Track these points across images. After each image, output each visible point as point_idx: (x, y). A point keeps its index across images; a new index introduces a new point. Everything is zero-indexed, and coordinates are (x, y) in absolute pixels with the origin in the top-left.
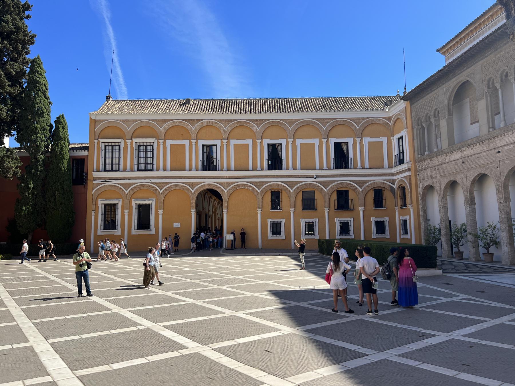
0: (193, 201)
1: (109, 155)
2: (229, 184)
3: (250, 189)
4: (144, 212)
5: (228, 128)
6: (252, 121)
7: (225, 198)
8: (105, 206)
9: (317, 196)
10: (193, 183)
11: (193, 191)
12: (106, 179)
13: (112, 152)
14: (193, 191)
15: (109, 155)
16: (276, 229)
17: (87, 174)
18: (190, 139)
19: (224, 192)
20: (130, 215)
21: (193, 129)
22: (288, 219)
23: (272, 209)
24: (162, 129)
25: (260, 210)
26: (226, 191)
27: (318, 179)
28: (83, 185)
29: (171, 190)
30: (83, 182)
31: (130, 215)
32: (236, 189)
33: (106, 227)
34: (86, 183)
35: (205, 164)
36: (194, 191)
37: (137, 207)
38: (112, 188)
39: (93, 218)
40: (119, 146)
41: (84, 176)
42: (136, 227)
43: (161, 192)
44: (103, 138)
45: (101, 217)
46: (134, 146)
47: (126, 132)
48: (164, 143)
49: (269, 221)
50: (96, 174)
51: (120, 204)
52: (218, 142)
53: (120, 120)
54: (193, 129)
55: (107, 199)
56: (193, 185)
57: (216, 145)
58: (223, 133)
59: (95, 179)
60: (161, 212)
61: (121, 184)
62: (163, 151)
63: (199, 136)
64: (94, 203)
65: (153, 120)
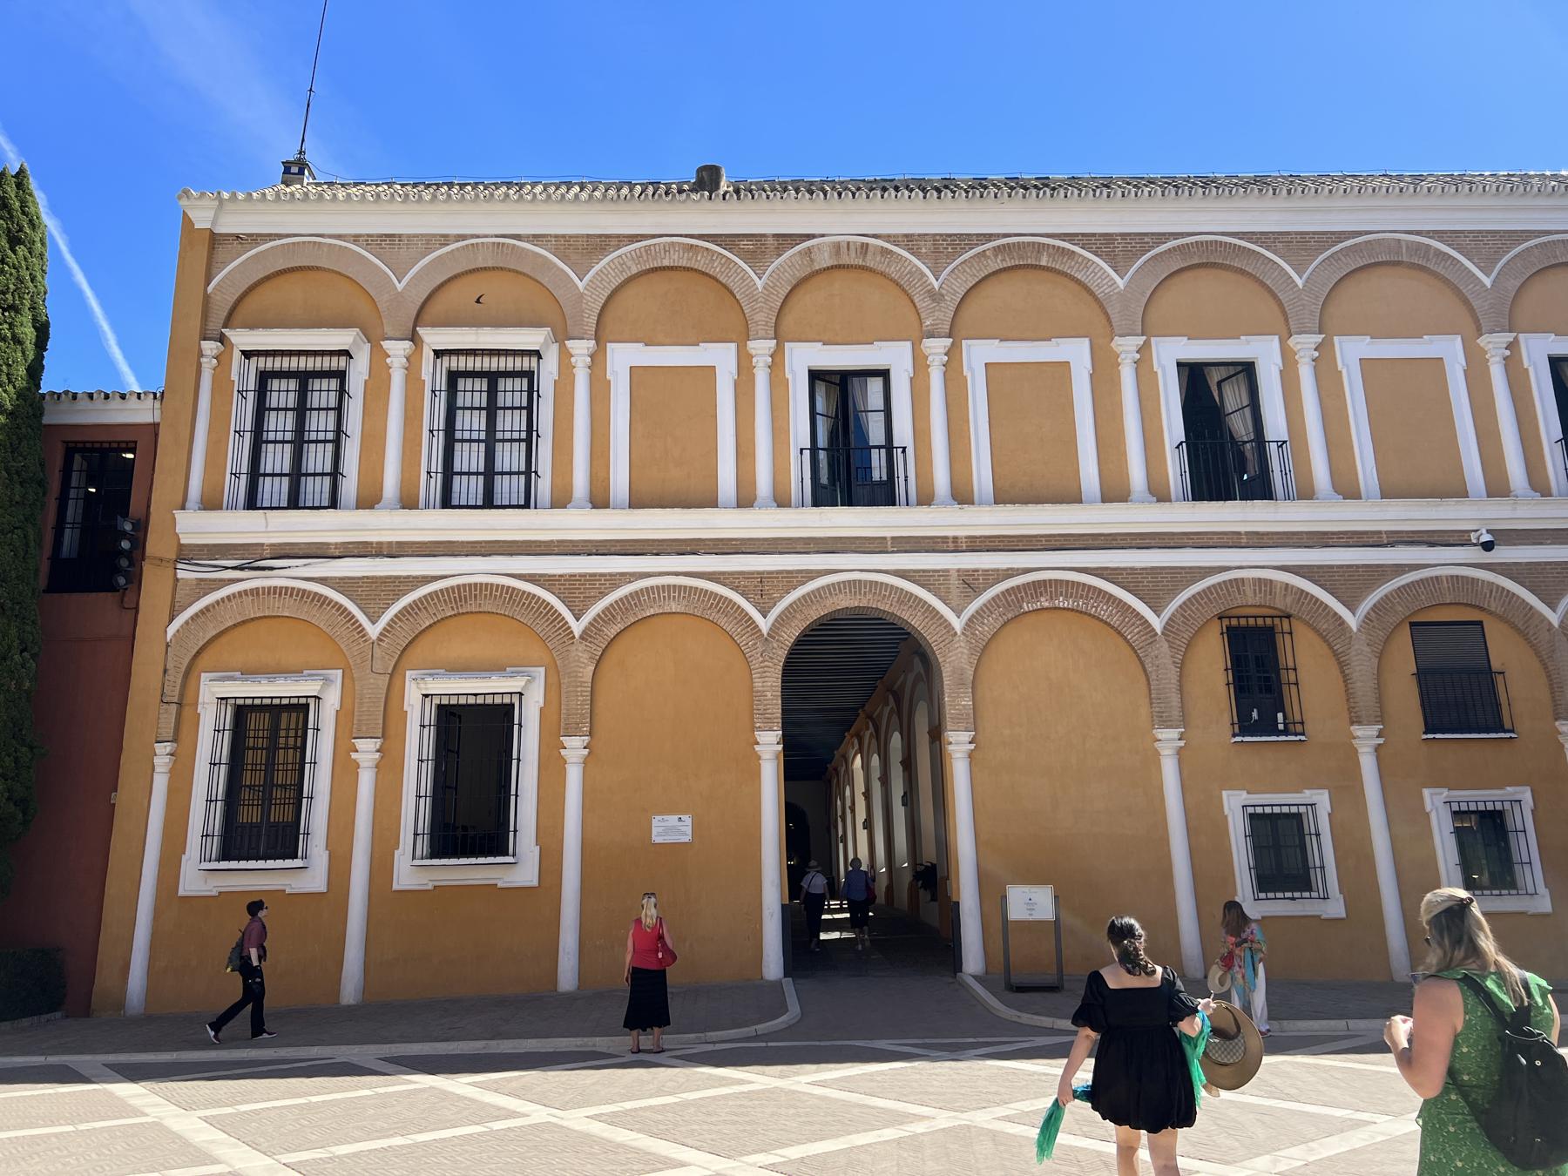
0: (770, 684)
1: (280, 424)
2: (972, 583)
3: (1104, 611)
4: (474, 746)
5: (948, 280)
6: (1085, 239)
7: (953, 661)
8: (242, 712)
9: (1503, 650)
10: (762, 577)
11: (764, 624)
12: (252, 557)
13: (301, 410)
14: (764, 624)
15: (280, 424)
16: (1281, 850)
17: (142, 526)
18: (741, 335)
19: (950, 624)
20: (389, 764)
21: (759, 282)
22: (1347, 788)
23: (1243, 732)
24: (587, 285)
25: (1173, 734)
26: (957, 624)
27: (1503, 554)
28: (112, 588)
29: (637, 617)
30: (118, 570)
31: (389, 764)
32: (1027, 605)
33: (237, 841)
34: (136, 580)
35: (824, 479)
36: (774, 624)
37: (430, 716)
38: (287, 608)
39: (160, 783)
40: (341, 375)
41: (124, 535)
42: (423, 845)
43: (577, 627)
44: (252, 326)
45: (207, 781)
46: (426, 375)
47: (383, 301)
48: (597, 360)
49: (1235, 805)
50: (194, 526)
51: (332, 700)
52: (895, 356)
53: (356, 238)
54: (759, 282)
55: (249, 672)
56: (762, 588)
57: (884, 374)
58: (923, 303)
59: (187, 554)
60: (574, 748)
61: (342, 584)
62: (594, 393)
63: (789, 321)
64: (173, 693)
65: (536, 238)
